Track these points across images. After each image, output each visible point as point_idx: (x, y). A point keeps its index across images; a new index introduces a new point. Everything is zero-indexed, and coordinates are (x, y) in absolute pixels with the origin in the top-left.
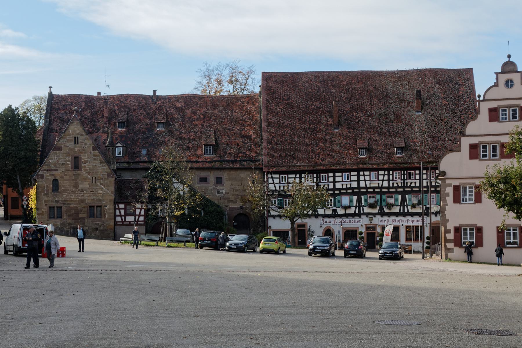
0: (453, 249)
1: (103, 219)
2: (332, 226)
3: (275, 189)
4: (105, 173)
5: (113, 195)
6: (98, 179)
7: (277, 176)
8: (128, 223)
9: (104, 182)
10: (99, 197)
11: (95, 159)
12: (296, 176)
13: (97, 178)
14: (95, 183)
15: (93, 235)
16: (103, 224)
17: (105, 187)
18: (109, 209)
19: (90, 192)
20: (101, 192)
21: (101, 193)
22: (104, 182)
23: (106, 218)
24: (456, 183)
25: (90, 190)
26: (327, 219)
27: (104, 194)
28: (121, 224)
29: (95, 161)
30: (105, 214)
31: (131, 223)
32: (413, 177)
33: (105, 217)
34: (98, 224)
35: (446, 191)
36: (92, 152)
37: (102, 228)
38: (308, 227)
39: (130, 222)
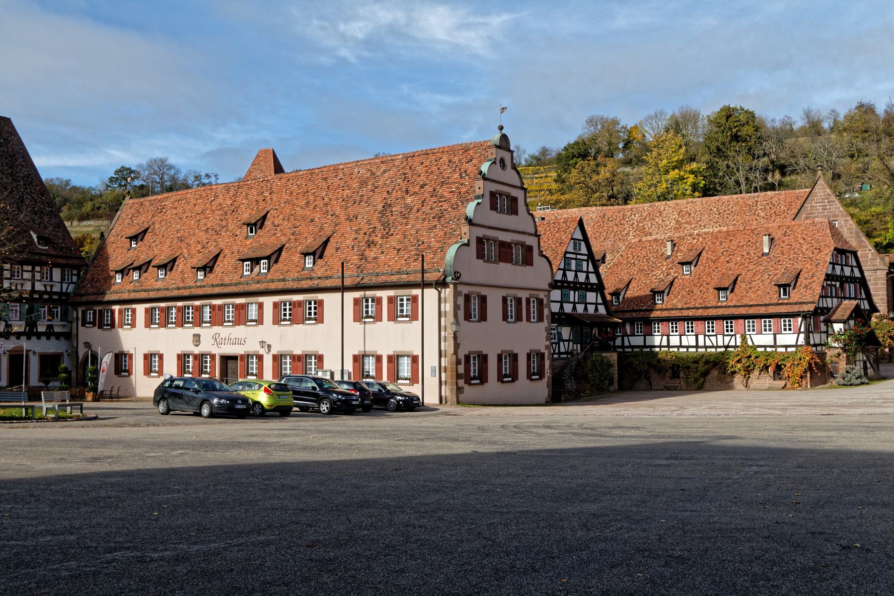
0: (463, 387)
24: (465, 290)
35: (458, 303)
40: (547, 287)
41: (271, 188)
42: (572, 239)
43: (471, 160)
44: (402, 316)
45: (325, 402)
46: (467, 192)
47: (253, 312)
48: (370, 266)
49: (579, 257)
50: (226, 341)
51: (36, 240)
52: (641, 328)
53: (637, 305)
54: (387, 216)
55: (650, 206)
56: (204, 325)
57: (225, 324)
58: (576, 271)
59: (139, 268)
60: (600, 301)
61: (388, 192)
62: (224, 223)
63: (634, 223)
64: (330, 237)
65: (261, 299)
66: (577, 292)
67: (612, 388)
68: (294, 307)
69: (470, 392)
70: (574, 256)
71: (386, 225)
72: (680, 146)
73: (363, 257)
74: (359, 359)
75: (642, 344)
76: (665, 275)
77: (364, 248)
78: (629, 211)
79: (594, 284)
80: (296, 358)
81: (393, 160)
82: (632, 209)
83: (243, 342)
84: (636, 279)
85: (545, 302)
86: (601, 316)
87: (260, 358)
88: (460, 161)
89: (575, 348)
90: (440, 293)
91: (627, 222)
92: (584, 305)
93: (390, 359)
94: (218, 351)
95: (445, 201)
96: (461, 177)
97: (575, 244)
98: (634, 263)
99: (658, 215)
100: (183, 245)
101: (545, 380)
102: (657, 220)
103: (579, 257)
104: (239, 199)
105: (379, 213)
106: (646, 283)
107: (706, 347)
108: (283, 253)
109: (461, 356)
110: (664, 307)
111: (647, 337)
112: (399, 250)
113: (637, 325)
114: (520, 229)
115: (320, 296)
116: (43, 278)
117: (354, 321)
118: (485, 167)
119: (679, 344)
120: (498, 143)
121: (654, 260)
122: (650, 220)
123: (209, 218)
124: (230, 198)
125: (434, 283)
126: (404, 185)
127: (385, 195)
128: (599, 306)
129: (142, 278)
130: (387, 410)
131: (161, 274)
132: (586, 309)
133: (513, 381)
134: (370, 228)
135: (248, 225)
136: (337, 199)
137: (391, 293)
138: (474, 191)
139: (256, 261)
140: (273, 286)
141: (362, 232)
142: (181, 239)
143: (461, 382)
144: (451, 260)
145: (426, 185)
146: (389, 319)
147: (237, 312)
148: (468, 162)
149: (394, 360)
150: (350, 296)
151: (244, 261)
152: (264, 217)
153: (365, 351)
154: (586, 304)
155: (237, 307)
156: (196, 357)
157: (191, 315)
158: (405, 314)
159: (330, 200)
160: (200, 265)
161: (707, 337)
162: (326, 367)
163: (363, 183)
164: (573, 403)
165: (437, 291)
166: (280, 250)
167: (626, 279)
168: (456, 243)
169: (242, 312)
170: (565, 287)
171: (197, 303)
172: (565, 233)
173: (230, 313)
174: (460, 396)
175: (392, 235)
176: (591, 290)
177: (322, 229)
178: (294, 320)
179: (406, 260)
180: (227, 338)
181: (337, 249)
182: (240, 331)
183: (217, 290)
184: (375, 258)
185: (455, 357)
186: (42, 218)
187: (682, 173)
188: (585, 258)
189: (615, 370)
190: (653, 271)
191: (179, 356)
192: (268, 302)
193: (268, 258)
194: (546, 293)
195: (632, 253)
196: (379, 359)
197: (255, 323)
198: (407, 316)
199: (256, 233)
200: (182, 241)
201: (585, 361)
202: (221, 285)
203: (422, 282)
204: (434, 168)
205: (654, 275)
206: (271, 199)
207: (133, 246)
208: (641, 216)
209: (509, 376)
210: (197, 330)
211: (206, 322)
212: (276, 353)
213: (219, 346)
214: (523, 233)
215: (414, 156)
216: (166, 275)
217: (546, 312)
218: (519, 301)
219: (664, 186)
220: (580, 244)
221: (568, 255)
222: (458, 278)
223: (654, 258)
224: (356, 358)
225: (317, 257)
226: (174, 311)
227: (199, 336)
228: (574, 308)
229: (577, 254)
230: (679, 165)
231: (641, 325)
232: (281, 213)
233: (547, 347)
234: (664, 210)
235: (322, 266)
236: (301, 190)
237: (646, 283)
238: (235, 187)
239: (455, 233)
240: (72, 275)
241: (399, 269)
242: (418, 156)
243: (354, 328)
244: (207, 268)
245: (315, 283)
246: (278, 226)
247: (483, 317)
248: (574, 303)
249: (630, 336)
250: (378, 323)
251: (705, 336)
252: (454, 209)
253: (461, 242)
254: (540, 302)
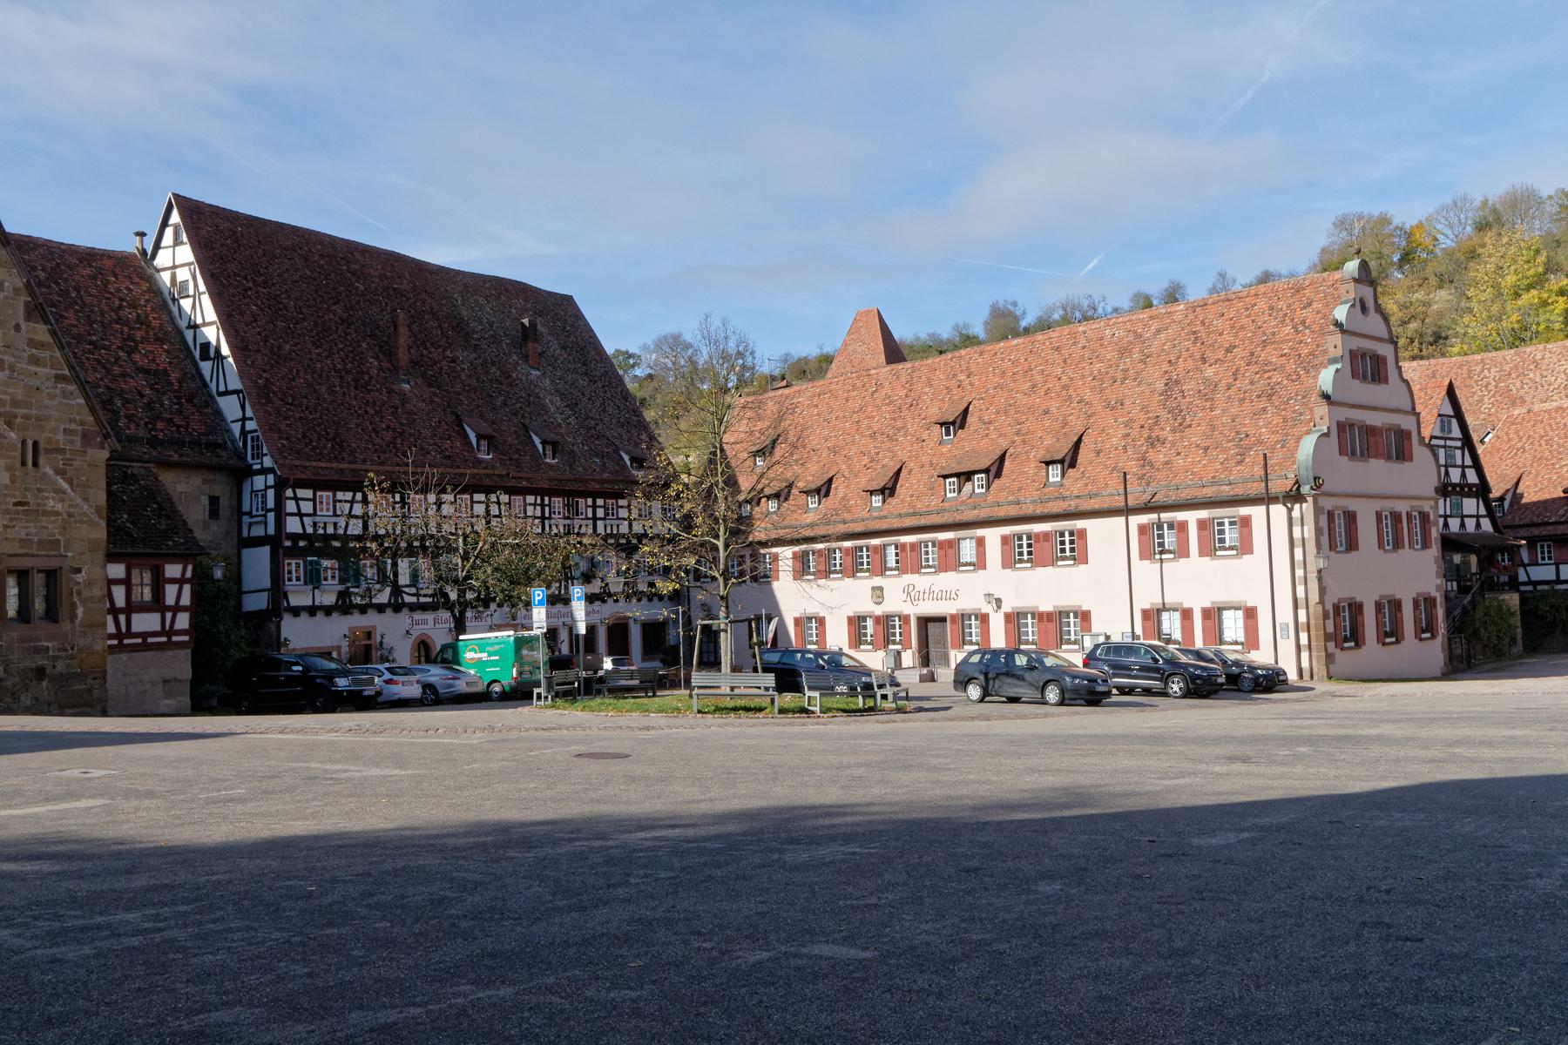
1: (66, 626)
2: (429, 633)
3: (301, 532)
4: (73, 426)
5: (103, 523)
6: (47, 451)
7: (308, 493)
8: (140, 640)
9: (68, 462)
10: (52, 529)
11: (34, 360)
12: (354, 496)
13: (42, 446)
14: (35, 464)
15: (26, 699)
16: (65, 650)
17: (72, 487)
18: (89, 584)
19: (16, 504)
20: (59, 507)
21: (57, 513)
22: (68, 462)
23: (78, 621)
24: (1327, 503)
25: (13, 496)
26: (418, 616)
27: (70, 515)
28: (140, 644)
29: (39, 369)
30: (73, 606)
31: (150, 640)
32: (613, 515)
33: (73, 616)
34: (48, 647)
35: (1321, 525)
36: (23, 327)
37: (61, 667)
38: (379, 639)
39: (144, 635)
40: (1432, 493)
41: (968, 368)
42: (1440, 415)
43: (1310, 305)
44: (1225, 549)
45: (1176, 680)
46: (1312, 354)
47: (968, 551)
48: (1161, 475)
49: (1449, 443)
50: (926, 595)
51: (628, 463)
52: (1549, 552)
53: (1538, 516)
54: (1176, 398)
55: (1516, 354)
56: (887, 573)
57: (923, 571)
58: (1446, 466)
59: (777, 496)
60: (1483, 511)
61: (1170, 362)
62: (899, 423)
63: (1489, 384)
64: (1082, 435)
65: (980, 532)
66: (1448, 499)
67: (1515, 650)
68: (1037, 541)
69: (1347, 659)
70: (1442, 442)
71: (1176, 412)
72: (1538, 252)
73: (1144, 461)
74: (1152, 616)
75: (1554, 578)
77: (1144, 448)
78: (1477, 364)
79: (1474, 485)
80: (1041, 617)
81: (1170, 313)
82: (1482, 361)
83: (953, 595)
84: (1530, 473)
85: (1432, 518)
86: (1486, 536)
87: (984, 619)
88: (1289, 306)
89: (1449, 588)
90: (1290, 510)
91: (1476, 382)
93: (1207, 613)
94: (914, 610)
95: (1275, 370)
96: (1297, 332)
97: (1442, 421)
98: (1523, 447)
99: (1532, 367)
100: (839, 459)
101: (1439, 639)
102: (1531, 375)
103: (1449, 443)
104: (918, 387)
105: (1161, 394)
106: (1550, 479)
108: (1007, 463)
109: (1329, 607)
111: (1561, 566)
112: (1206, 449)
113: (1542, 547)
114: (1393, 405)
115: (1080, 524)
116: (608, 514)
117: (1200, 556)
118: (1341, 313)
119: (1554, 578)
120: (1356, 275)
121: (1561, 441)
122: (1518, 376)
123: (873, 417)
124: (903, 386)
125: (1280, 496)
126: (1196, 350)
127: (1165, 367)
128: (1481, 519)
129: (782, 509)
130: (1239, 690)
131: (812, 503)
132: (1463, 525)
133: (1398, 642)
134: (1149, 418)
135: (942, 424)
136: (1083, 377)
137: (1204, 514)
138: (1326, 352)
139: (967, 476)
140: (1001, 513)
141: (1137, 425)
142: (834, 450)
143: (1331, 645)
144: (1307, 460)
145: (1235, 347)
146: (1202, 554)
147: (943, 552)
148: (1305, 308)
149: (1213, 615)
150: (1137, 520)
151: (945, 477)
152: (966, 411)
153: (1164, 604)
154: (1463, 517)
155: (941, 545)
156: (877, 620)
157: (838, 562)
158: (1227, 545)
159: (1072, 379)
160: (877, 485)
162: (1095, 630)
163: (1124, 351)
164: (1465, 675)
165: (1285, 508)
166: (1002, 458)
168: (1308, 432)
169: (950, 551)
171: (876, 542)
172: (1426, 407)
173: (932, 554)
174: (1331, 667)
175: (1190, 426)
176: (1469, 496)
177: (1065, 424)
178: (1036, 560)
179: (1221, 464)
180: (927, 591)
181: (1099, 452)
182: (948, 580)
183: (908, 523)
184: (1167, 463)
185: (1320, 608)
186: (630, 432)
187: (1545, 295)
188: (1459, 444)
189: (1517, 621)
190: (1562, 459)
191: (850, 620)
192: (993, 536)
193: (987, 471)
194: (1432, 503)
195: (1517, 432)
196: (1187, 614)
197: (972, 568)
198: (1231, 548)
199: (955, 435)
200: (835, 453)
201: (1474, 609)
202: (915, 514)
203: (1265, 496)
204: (1245, 321)
206: (971, 384)
207: (758, 464)
208: (1501, 370)
209: (1391, 633)
210: (878, 581)
211: (891, 570)
212: (1010, 610)
213: (915, 603)
214: (1397, 411)
215: (1205, 305)
216: (819, 504)
217: (1435, 533)
218: (1396, 517)
219: (1515, 318)
220: (1450, 423)
222: (1319, 487)
223: (1561, 438)
224: (1146, 614)
225: (1066, 464)
226: (891, 551)
227: (881, 589)
229: (1446, 439)
230: (1538, 282)
231: (1549, 546)
232: (992, 405)
233: (1438, 588)
234: (1543, 358)
235: (1077, 479)
236: (1019, 368)
237: (1550, 479)
238: (907, 370)
239: (1302, 418)
240: (618, 507)
241: (1213, 477)
242: (1213, 304)
243: (1146, 571)
244: (888, 491)
245: (1071, 505)
246: (990, 423)
247: (1352, 545)
249: (1529, 565)
250: (1183, 560)
252: (1293, 381)
253: (1316, 431)
254: (1424, 517)
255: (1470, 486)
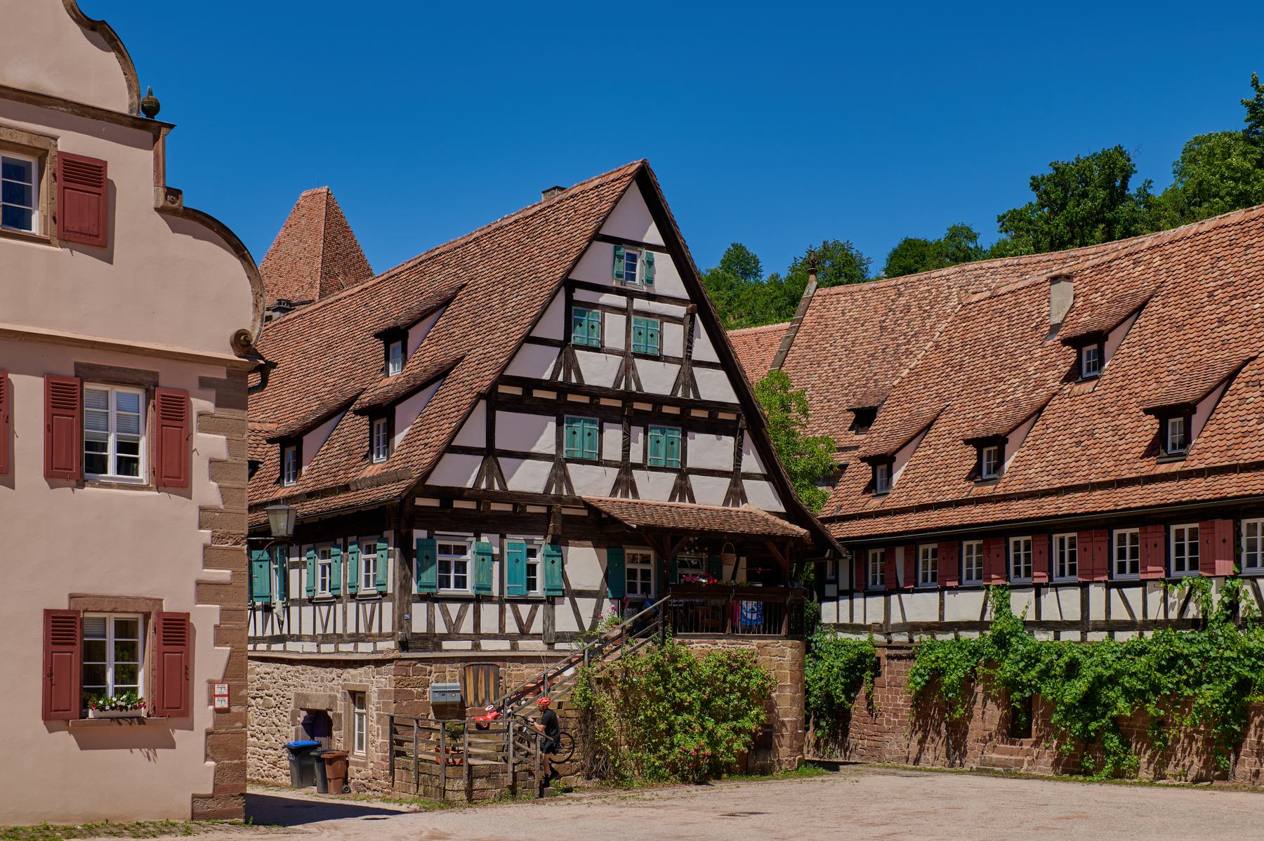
60: (751, 463)
76: (1030, 387)
79: (724, 406)
92: (672, 477)
107: (1111, 627)
110: (1000, 491)
128: (747, 484)
132: (682, 491)
161: (1114, 592)
167: (927, 413)
170: (578, 409)
176: (714, 426)
190: (1001, 380)
205: (1000, 392)
221: (580, 295)
228: (625, 484)
248: (626, 467)
249: (907, 591)
251: (1109, 586)
255: (715, 407)
